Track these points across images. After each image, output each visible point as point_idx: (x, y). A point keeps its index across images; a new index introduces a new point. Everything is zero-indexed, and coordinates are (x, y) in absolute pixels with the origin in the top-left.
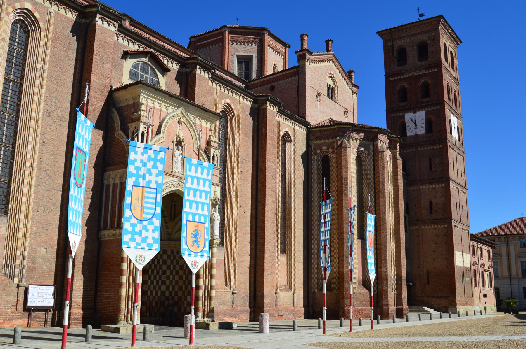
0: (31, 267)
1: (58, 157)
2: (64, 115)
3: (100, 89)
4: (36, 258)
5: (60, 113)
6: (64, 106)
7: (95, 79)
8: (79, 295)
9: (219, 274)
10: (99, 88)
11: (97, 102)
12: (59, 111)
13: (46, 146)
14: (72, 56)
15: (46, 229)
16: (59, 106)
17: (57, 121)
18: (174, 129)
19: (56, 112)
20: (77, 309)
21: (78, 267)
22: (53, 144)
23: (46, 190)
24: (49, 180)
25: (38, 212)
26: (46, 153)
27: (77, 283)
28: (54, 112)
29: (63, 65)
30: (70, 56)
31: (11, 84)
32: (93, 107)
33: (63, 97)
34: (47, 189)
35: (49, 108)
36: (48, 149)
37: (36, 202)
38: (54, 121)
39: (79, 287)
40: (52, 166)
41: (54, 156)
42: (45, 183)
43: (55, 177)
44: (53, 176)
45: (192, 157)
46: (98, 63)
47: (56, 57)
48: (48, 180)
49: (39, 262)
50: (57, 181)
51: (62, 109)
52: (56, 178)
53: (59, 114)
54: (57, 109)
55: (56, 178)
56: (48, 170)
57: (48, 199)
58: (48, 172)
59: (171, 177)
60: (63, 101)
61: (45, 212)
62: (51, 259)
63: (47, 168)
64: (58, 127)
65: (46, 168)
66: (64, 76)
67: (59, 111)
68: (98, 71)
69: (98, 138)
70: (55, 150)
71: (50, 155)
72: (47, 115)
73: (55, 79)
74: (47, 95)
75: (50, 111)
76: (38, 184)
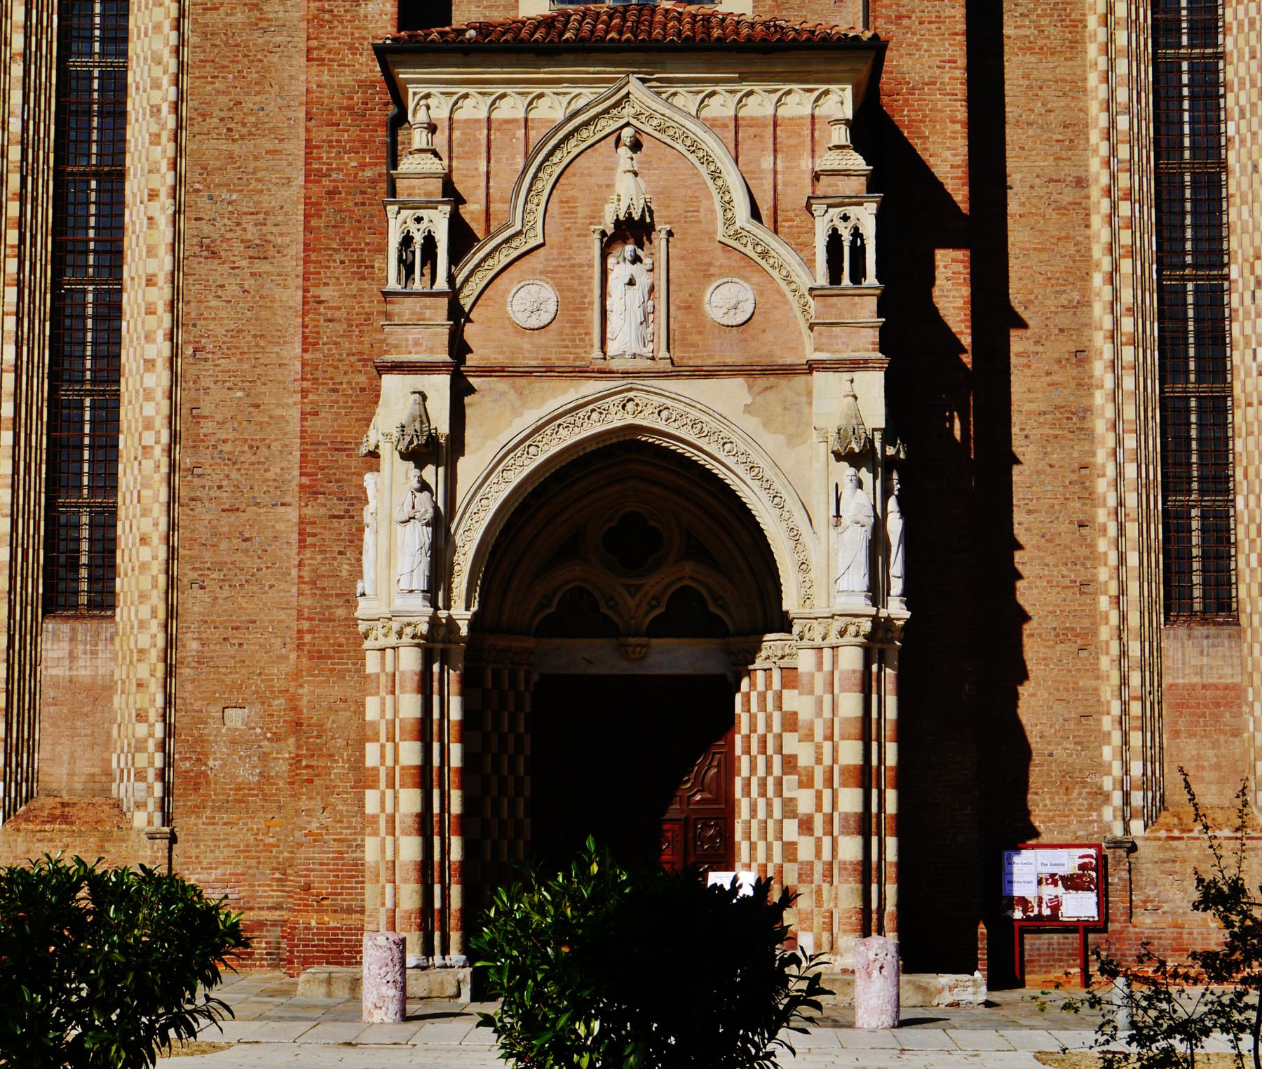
0: (192, 774)
1: (263, 389)
2: (269, 237)
3: (350, 108)
4: (207, 741)
5: (252, 233)
6: (265, 205)
7: (326, 77)
8: (321, 864)
9: (1211, 753)
10: (345, 102)
11: (342, 158)
12: (250, 227)
13: (210, 362)
14: (281, 14)
15: (234, 641)
16: (246, 210)
17: (244, 263)
18: (593, 181)
19: (239, 233)
20: (317, 912)
21: (307, 767)
22: (237, 348)
23: (223, 510)
24: (234, 475)
25: (202, 588)
26: (212, 385)
27: (309, 822)
28: (229, 235)
29: (246, 60)
30: (271, 16)
31: (93, 184)
32: (325, 181)
33: (259, 175)
34: (227, 507)
35: (206, 229)
36: (218, 369)
37: (191, 557)
38: (233, 268)
39: (321, 834)
40: (240, 423)
41: (243, 389)
42: (220, 487)
43: (254, 459)
44: (248, 457)
45: (713, 270)
46: (331, 11)
47: (218, 42)
48: (228, 476)
49: (218, 755)
50: (266, 470)
51: (261, 216)
52: (259, 463)
53: (249, 237)
54: (238, 224)
55: (259, 463)
56: (224, 442)
57: (235, 541)
58: (227, 447)
59: (591, 382)
60: (260, 186)
61: (227, 587)
62: (266, 743)
63: (222, 435)
64: (250, 283)
65: (218, 436)
66: (258, 99)
67: (250, 227)
68: (334, 44)
69: (361, 290)
70: (246, 366)
71: (229, 389)
72: (205, 253)
73: (222, 120)
74: (197, 186)
75: (214, 236)
76: (192, 495)
